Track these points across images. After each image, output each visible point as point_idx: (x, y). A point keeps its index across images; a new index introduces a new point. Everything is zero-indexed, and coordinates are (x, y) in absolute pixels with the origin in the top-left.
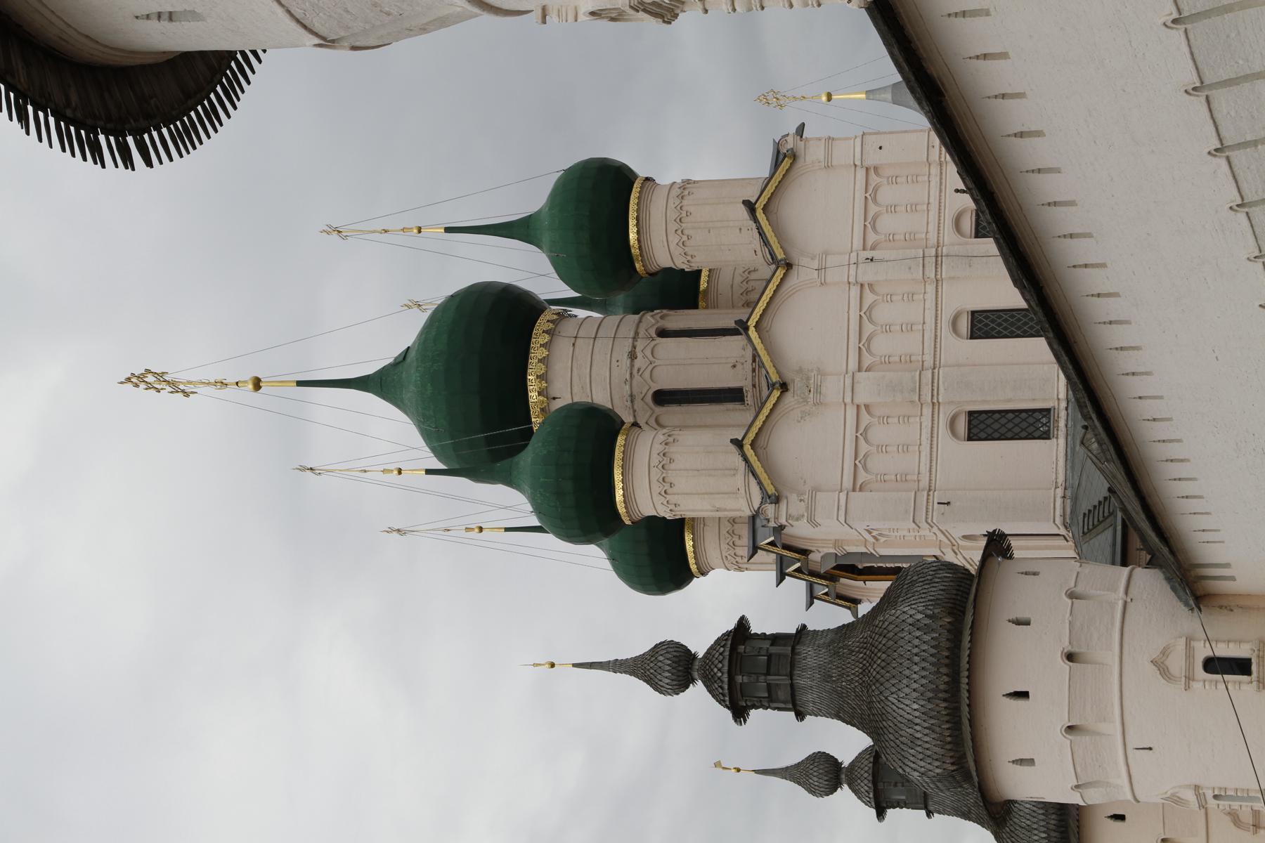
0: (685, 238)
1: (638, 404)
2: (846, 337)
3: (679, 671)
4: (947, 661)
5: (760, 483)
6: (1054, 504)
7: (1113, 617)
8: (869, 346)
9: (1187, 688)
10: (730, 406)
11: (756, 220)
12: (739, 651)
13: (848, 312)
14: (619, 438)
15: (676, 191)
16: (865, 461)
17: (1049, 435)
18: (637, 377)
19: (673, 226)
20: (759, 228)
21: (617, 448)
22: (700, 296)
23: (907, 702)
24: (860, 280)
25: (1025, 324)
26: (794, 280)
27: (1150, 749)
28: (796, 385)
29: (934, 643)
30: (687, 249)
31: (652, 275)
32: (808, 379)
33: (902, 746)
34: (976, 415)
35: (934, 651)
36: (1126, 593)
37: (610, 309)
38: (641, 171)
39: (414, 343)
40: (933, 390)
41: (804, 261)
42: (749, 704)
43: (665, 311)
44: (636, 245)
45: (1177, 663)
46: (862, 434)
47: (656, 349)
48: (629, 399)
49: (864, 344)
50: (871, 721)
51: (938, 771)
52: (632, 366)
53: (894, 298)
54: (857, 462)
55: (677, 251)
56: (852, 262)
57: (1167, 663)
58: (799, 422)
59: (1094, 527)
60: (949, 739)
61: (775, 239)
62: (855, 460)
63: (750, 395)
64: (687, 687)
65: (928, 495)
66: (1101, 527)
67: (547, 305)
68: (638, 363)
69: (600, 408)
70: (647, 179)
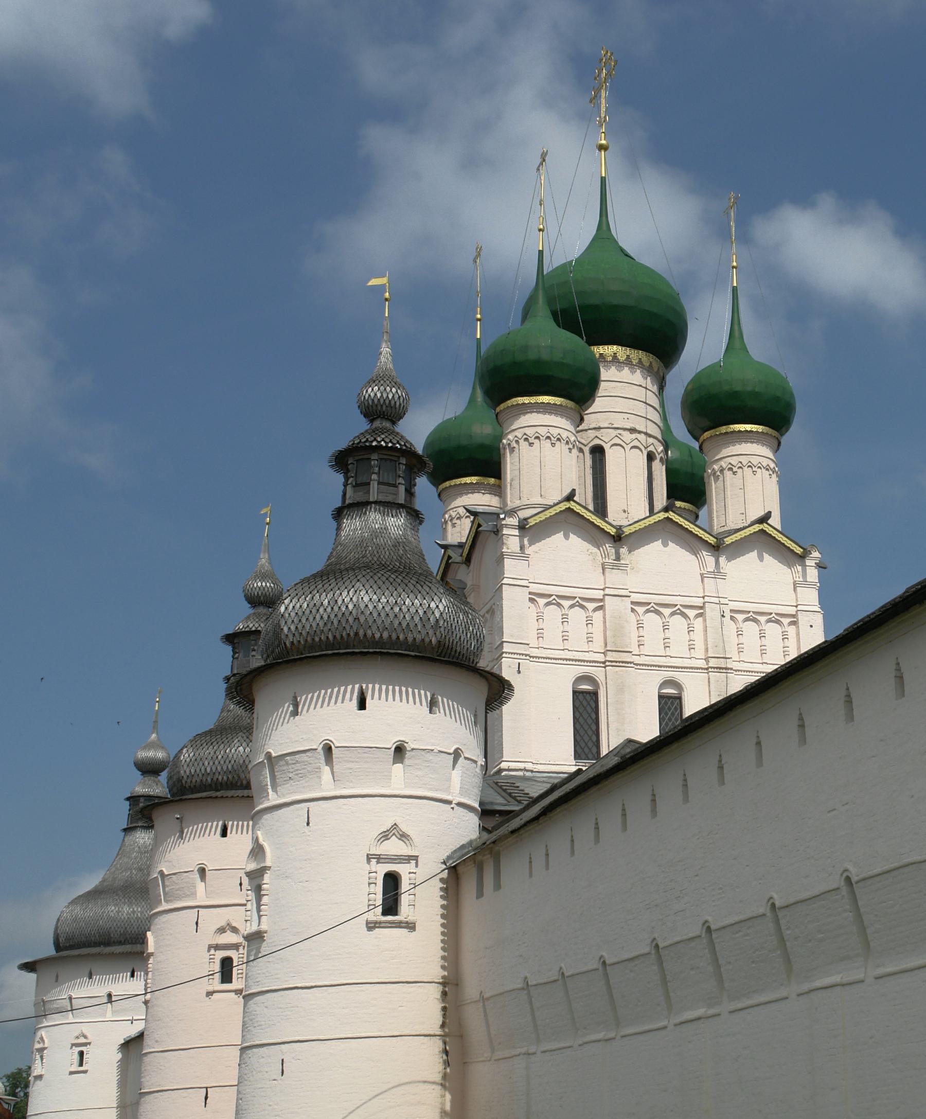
1: (592, 434)
4: (394, 637)
6: (518, 762)
12: (401, 458)
29: (412, 626)
35: (404, 625)
36: (460, 804)
40: (616, 662)
44: (729, 430)
45: (394, 847)
46: (579, 603)
48: (597, 426)
52: (625, 429)
58: (588, 550)
59: (505, 790)
60: (317, 639)
66: (503, 794)
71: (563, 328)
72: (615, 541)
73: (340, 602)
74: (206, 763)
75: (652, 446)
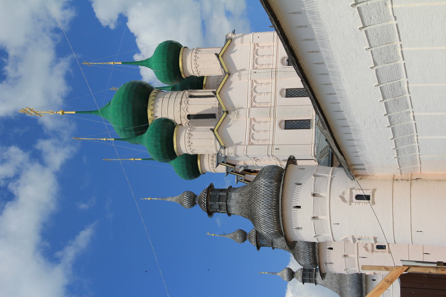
0: (197, 66)
1: (183, 119)
3: (191, 200)
4: (275, 197)
5: (219, 143)
6: (311, 148)
7: (327, 182)
8: (254, 99)
9: (350, 204)
11: (219, 60)
12: (210, 194)
16: (253, 135)
17: (310, 128)
18: (182, 110)
20: (220, 63)
22: (203, 86)
23: (262, 210)
25: (303, 93)
27: (338, 224)
29: (271, 191)
30: (198, 69)
31: (187, 78)
33: (261, 224)
34: (287, 121)
35: (271, 193)
38: (184, 45)
40: (274, 113)
42: (213, 211)
43: (191, 90)
44: (182, 68)
45: (347, 197)
48: (180, 117)
50: (251, 216)
51: (272, 232)
53: (262, 84)
54: (250, 136)
55: (195, 70)
56: (249, 73)
57: (344, 196)
60: (276, 221)
61: (225, 65)
62: (249, 135)
64: (194, 206)
65: (272, 146)
67: (155, 88)
68: (182, 106)
70: (185, 47)
71: (147, 130)
72: (228, 113)
73: (263, 214)
74: (306, 255)
75: (187, 96)
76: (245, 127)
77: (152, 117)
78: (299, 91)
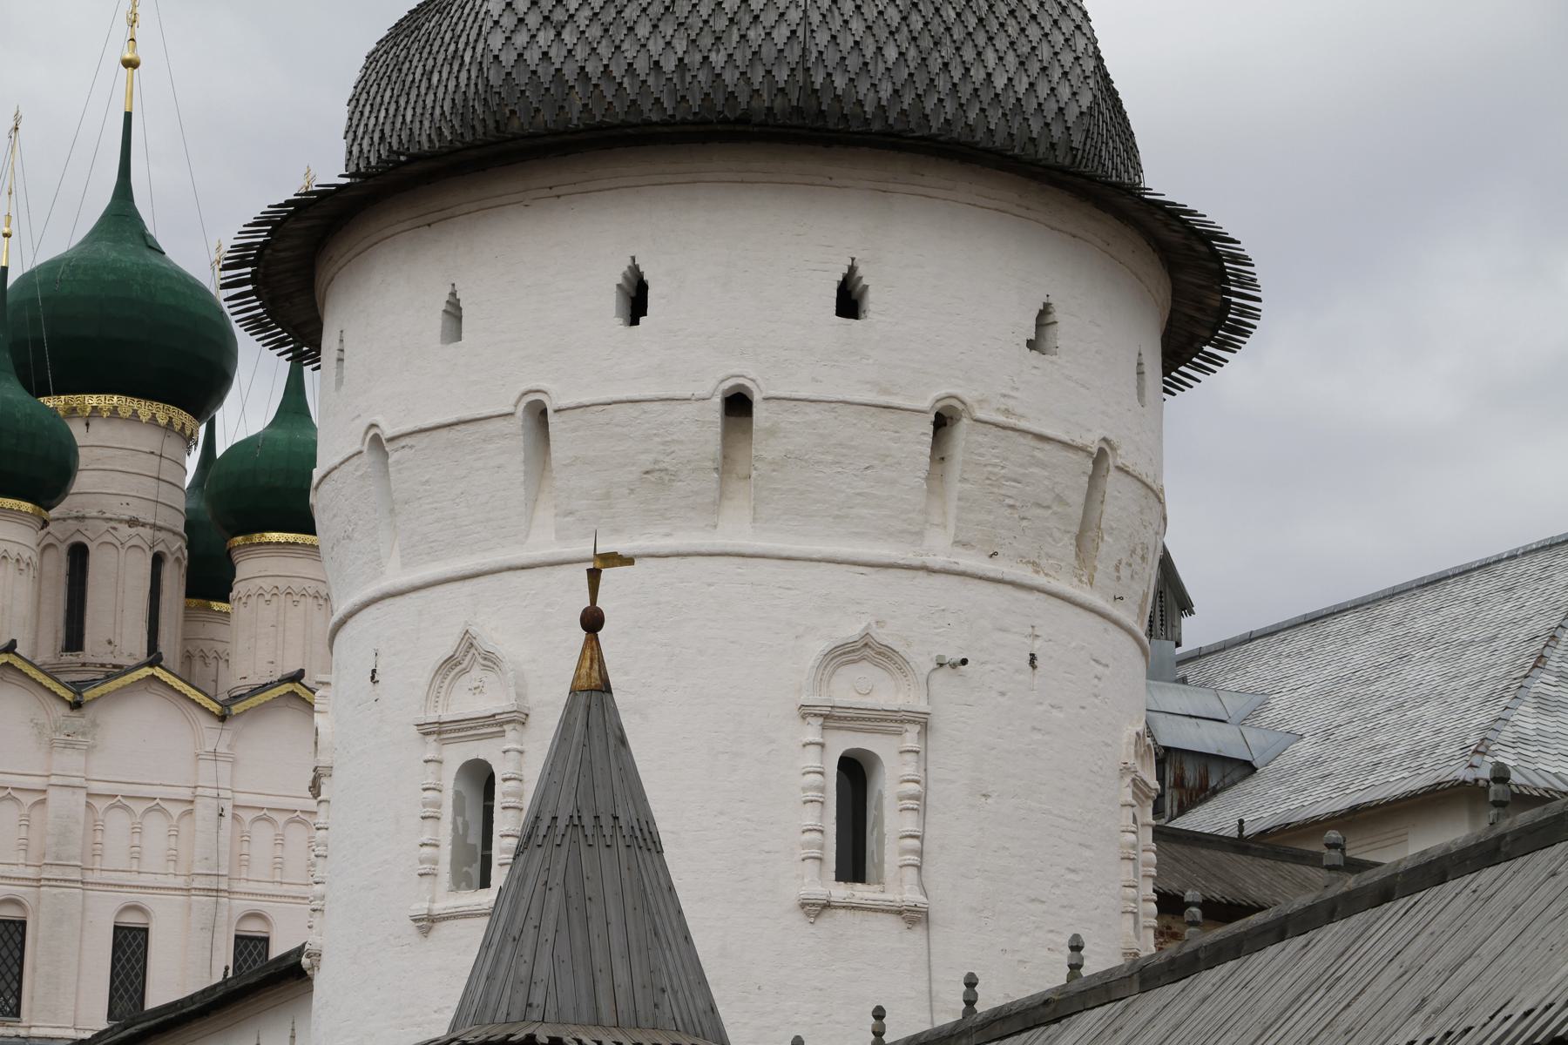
0: (268, 597)
1: (72, 525)
2: (130, 781)
8: (117, 807)
10: (62, 634)
11: (282, 681)
13: (160, 784)
14: (29, 505)
15: (323, 591)
19: (282, 584)
21: (17, 502)
22: (204, 601)
24: (198, 800)
25: (127, 991)
26: (205, 722)
28: (77, 720)
32: (84, 734)
34: (20, 929)
37: (197, 492)
39: (169, 261)
40: (56, 880)
41: (227, 737)
43: (185, 563)
44: (264, 540)
47: (139, 550)
48: (80, 514)
49: (118, 802)
52: (121, 521)
53: (173, 839)
55: (253, 586)
58: (32, 721)
63: (74, 659)
69: (71, 481)
76: (13, 771)
77: (89, 409)
78: (137, 976)
